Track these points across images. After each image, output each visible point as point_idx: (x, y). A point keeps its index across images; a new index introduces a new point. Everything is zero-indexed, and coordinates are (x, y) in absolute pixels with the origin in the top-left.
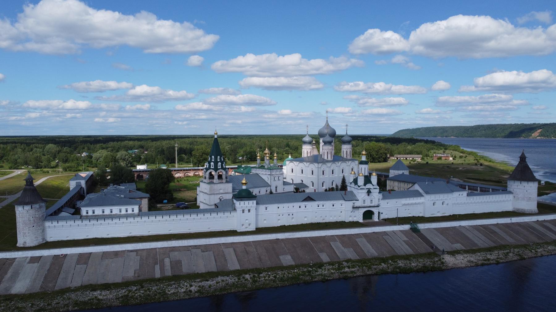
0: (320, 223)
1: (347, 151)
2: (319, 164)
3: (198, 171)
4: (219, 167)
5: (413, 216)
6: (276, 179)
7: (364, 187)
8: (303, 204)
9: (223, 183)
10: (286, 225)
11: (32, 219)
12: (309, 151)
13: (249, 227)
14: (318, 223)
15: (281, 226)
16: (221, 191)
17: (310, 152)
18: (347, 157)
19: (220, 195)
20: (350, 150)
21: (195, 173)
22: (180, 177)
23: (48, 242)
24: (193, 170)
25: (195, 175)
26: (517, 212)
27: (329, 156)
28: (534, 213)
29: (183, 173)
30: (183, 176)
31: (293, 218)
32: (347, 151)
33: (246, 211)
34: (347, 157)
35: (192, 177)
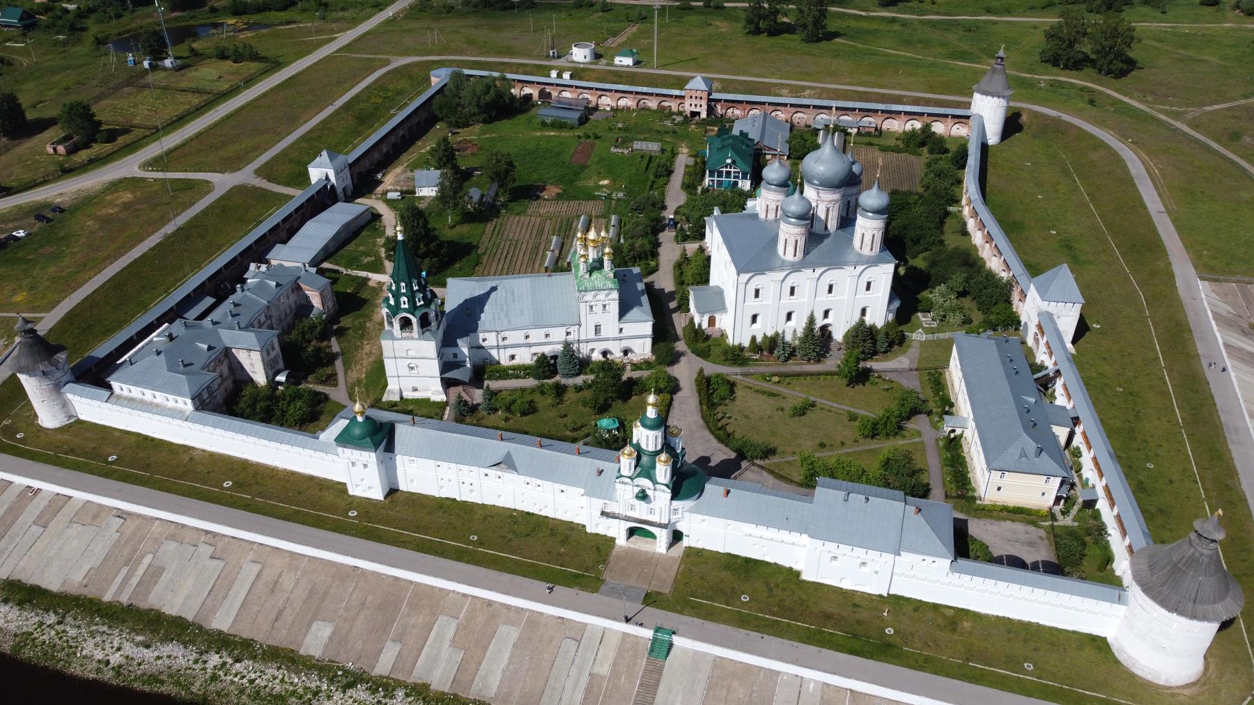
0: (533, 514)
1: (863, 234)
2: (742, 275)
3: (669, 99)
4: (405, 303)
5: (775, 563)
6: (598, 309)
7: (629, 480)
8: (493, 472)
9: (412, 338)
10: (458, 499)
11: (37, 391)
12: (773, 206)
13: (368, 492)
14: (528, 513)
15: (447, 498)
16: (412, 353)
17: (775, 207)
18: (861, 248)
19: (410, 361)
20: (875, 232)
21: (663, 103)
22: (628, 108)
23: (80, 422)
24: (657, 95)
25: (661, 109)
26: (1116, 654)
27: (790, 249)
28: (1162, 683)
29: (635, 98)
30: (635, 107)
31: (471, 491)
32: (863, 234)
33: (360, 466)
34: (861, 248)
35: (654, 111)
